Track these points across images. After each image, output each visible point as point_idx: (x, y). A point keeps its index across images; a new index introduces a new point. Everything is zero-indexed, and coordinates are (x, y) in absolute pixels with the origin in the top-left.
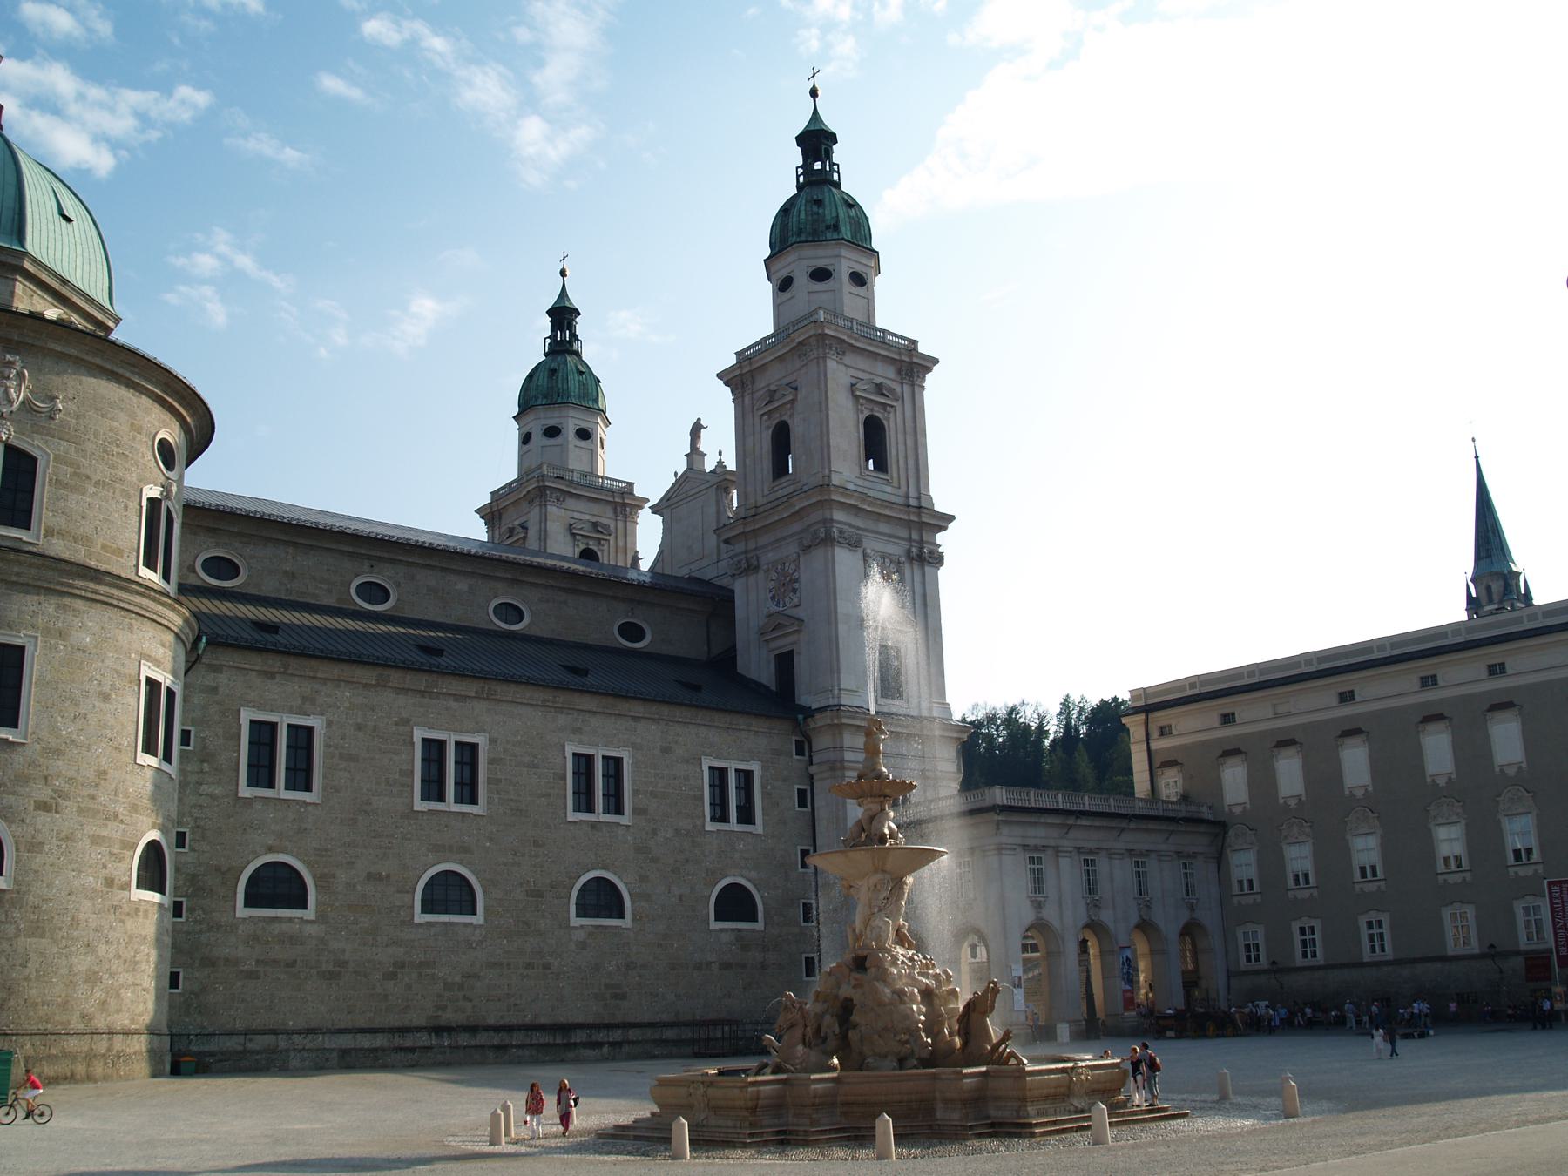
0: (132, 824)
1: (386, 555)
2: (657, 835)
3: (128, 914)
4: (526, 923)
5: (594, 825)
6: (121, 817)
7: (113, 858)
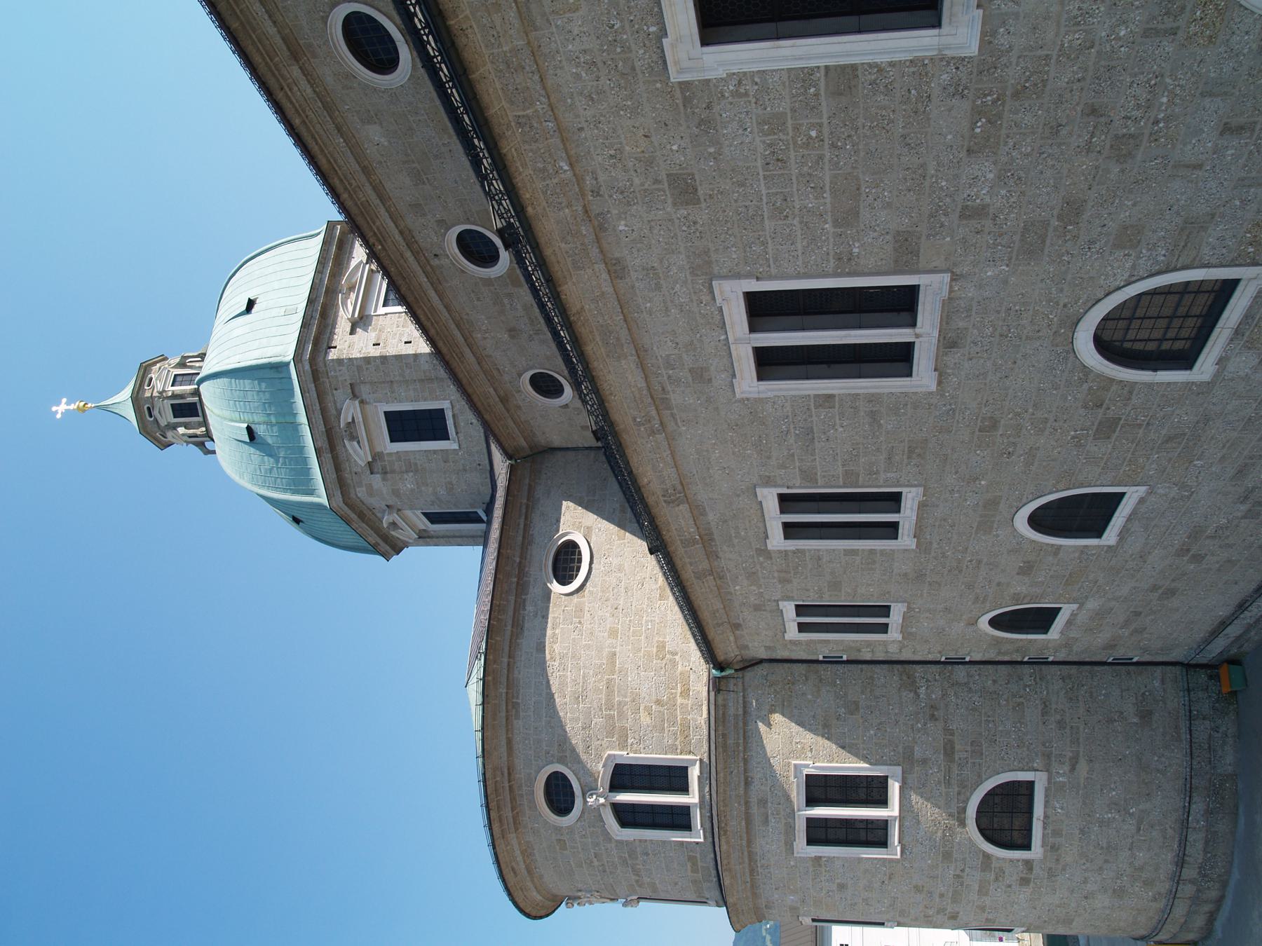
0: (964, 859)
1: (408, 254)
2: (984, 207)
3: (1057, 860)
4: (1169, 439)
5: (949, 343)
6: (958, 872)
7: (1001, 879)
